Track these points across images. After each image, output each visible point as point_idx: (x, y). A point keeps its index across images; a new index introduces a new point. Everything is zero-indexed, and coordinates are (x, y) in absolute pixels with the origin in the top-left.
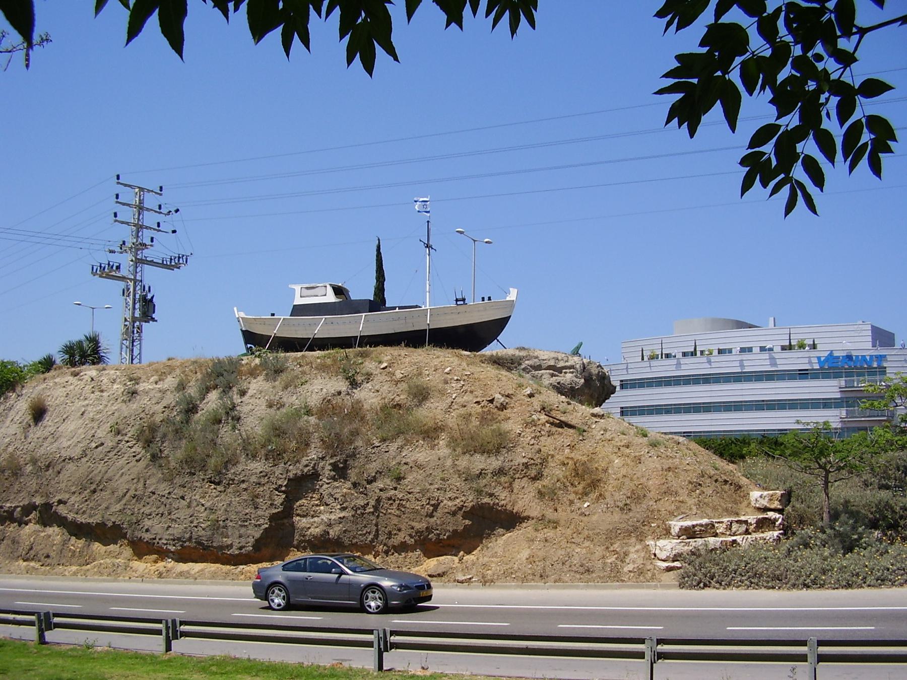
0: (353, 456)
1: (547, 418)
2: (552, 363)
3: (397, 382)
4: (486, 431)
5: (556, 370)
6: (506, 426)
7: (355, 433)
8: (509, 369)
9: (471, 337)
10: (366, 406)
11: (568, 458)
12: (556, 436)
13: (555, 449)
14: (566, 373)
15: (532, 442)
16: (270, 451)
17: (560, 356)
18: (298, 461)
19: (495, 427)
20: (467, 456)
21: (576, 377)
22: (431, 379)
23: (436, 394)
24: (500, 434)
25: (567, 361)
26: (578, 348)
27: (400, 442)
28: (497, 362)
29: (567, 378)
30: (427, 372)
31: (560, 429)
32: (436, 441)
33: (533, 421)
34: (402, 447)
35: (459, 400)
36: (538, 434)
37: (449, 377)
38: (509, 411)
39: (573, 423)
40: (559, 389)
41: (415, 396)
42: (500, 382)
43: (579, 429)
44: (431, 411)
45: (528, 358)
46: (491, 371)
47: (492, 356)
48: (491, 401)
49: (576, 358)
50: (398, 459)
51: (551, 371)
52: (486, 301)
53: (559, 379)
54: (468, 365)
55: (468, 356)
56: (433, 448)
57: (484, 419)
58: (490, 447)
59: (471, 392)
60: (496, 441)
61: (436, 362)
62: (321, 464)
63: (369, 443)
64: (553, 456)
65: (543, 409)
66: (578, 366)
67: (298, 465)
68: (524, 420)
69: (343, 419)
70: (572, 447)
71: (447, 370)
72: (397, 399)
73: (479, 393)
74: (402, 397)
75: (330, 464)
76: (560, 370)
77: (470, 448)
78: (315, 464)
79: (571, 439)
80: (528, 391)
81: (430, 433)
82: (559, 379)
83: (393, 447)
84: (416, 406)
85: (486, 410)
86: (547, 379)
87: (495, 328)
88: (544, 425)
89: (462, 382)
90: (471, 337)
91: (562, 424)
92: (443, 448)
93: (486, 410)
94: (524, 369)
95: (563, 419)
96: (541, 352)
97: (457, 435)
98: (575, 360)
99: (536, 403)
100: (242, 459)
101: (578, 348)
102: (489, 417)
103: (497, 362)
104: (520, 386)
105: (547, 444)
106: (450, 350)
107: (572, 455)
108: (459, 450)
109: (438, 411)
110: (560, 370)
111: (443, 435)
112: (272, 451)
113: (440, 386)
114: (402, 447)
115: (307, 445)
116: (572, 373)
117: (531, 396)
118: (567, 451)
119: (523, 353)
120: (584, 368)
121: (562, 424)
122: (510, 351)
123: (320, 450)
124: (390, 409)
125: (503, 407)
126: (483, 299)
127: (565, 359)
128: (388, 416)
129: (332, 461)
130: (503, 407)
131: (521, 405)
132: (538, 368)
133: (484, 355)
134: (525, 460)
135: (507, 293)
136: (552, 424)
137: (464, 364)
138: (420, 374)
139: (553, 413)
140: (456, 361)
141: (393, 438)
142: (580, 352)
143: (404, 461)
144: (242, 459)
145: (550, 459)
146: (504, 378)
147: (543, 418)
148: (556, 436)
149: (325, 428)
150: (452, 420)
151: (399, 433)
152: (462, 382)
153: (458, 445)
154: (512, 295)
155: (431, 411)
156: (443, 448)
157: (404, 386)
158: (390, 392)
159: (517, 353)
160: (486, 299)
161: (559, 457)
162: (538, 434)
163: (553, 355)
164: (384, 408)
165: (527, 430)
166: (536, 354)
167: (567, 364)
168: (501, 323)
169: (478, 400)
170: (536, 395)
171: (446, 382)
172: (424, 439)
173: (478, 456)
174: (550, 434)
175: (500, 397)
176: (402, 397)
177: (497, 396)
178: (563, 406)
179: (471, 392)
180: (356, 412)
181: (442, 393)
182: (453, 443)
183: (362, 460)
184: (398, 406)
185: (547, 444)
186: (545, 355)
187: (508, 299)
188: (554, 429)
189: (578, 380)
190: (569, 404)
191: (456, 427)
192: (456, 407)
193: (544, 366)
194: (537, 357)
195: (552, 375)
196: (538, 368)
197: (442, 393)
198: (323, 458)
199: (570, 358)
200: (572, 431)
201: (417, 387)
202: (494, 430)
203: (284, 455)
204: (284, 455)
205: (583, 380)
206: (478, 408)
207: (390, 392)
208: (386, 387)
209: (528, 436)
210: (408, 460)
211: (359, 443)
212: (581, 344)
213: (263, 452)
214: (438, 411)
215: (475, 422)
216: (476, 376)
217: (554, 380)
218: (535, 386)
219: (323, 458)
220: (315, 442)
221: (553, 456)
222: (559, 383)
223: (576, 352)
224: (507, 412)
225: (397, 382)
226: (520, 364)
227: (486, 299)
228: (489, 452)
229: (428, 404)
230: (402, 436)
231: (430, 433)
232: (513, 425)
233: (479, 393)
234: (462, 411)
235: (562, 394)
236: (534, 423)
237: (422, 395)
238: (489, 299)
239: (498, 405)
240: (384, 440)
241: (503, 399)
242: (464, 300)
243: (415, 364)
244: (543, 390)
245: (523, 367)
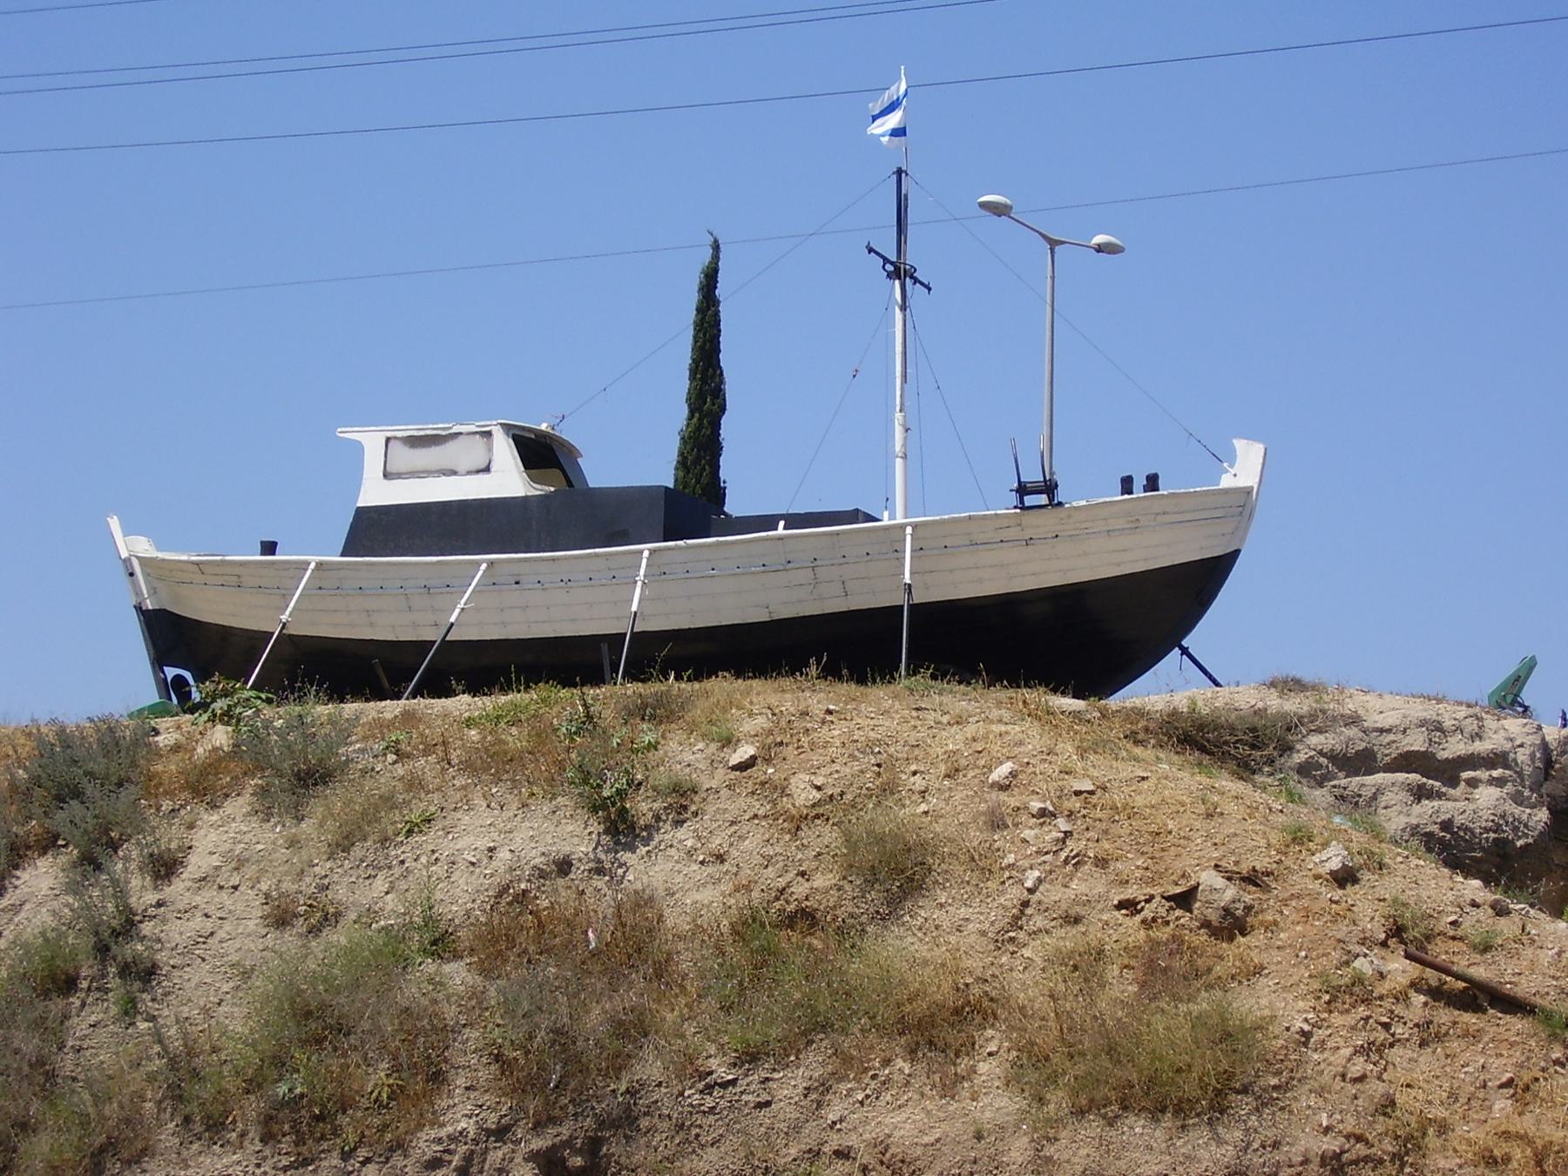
0: (626, 1121)
1: (1414, 970)
2: (1416, 742)
3: (798, 823)
4: (1171, 1025)
5: (1434, 771)
6: (1251, 1003)
7: (632, 1030)
8: (1245, 770)
9: (1080, 639)
10: (675, 920)
11: (1506, 1135)
12: (1455, 1045)
13: (1453, 1096)
14: (1473, 783)
15: (1358, 1067)
16: (283, 1104)
17: (1449, 715)
18: (399, 1146)
19: (1203, 1004)
20: (1093, 1127)
21: (1518, 799)
22: (937, 809)
23: (958, 869)
24: (1227, 1036)
25: (1477, 736)
26: (1518, 681)
27: (813, 1064)
28: (1197, 738)
29: (1482, 804)
30: (918, 782)
31: (1469, 1018)
32: (964, 1064)
33: (1358, 980)
34: (824, 1087)
35: (1052, 894)
36: (1381, 1035)
37: (1011, 800)
38: (1257, 938)
39: (1524, 987)
40: (1451, 849)
41: (872, 878)
42: (1218, 825)
43: (1548, 1017)
44: (942, 938)
45: (1319, 721)
46: (1176, 780)
47: (1175, 713)
48: (1184, 900)
49: (1514, 725)
50: (810, 1135)
51: (1414, 777)
52: (1139, 493)
53: (1446, 808)
54: (1082, 752)
55: (1076, 715)
56: (948, 1089)
57: (1160, 972)
58: (1190, 1089)
59: (1102, 862)
60: (1209, 1062)
61: (954, 740)
62: (496, 1156)
63: (691, 1070)
64: (1443, 1128)
65: (1397, 931)
66: (1522, 756)
67: (397, 1160)
68: (1322, 975)
69: (583, 970)
70: (1520, 1090)
71: (1001, 772)
72: (800, 889)
73: (1131, 865)
74: (820, 881)
75: (533, 1157)
76: (1449, 772)
77: (1105, 1090)
78: (468, 1158)
79: (1518, 1056)
80: (1333, 858)
81: (938, 1031)
82: (1446, 808)
83: (790, 1085)
84: (882, 918)
85: (1163, 934)
86: (1399, 808)
87: (1165, 605)
88: (1401, 997)
89: (1062, 823)
90: (1080, 639)
91: (1480, 997)
92: (991, 1094)
93: (1163, 934)
94: (1304, 770)
95: (1480, 972)
96: (1372, 701)
97: (1047, 1038)
98: (1507, 732)
99: (1367, 907)
100: (167, 1136)
101: (1518, 681)
102: (1178, 964)
103: (1197, 738)
104: (1300, 837)
105: (1420, 1078)
106: (1000, 693)
107: (1526, 1124)
108: (1058, 1101)
109: (970, 937)
110: (1449, 772)
111: (993, 1039)
112: (294, 1102)
113: (975, 837)
114: (824, 1087)
115: (437, 1078)
116: (1499, 782)
117: (1345, 877)
118: (1502, 1105)
119: (1294, 705)
120: (1549, 763)
121: (1480, 997)
122: (1243, 696)
123: (486, 1098)
124: (773, 934)
125: (1232, 925)
126: (1127, 485)
127: (1471, 726)
128: (765, 960)
129: (538, 1144)
130: (1232, 925)
131: (1307, 915)
132: (1362, 762)
133: (1140, 713)
134: (1331, 1144)
135: (1222, 458)
136: (1437, 994)
137: (1067, 748)
138: (889, 789)
139: (1440, 951)
140: (1034, 738)
141: (787, 1052)
142: (1527, 696)
143: (834, 1142)
144: (167, 1136)
145: (1432, 1140)
146: (1230, 807)
147: (1399, 968)
148: (1455, 1045)
149: (509, 1013)
150: (1027, 976)
151: (813, 1027)
152: (1062, 823)
153: (1053, 1079)
154: (1245, 467)
155: (942, 938)
156: (991, 1094)
157: (825, 836)
158: (769, 861)
159: (1274, 702)
160: (1139, 482)
161: (1471, 1132)
162: (1381, 1035)
163: (1419, 710)
164: (746, 927)
165: (1337, 1019)
166: (1350, 706)
167: (1480, 747)
168: (1201, 582)
169: (1130, 892)
170: (1365, 876)
171: (997, 822)
172: (912, 1053)
173: (1136, 1126)
174: (1428, 1036)
175: (1219, 882)
176: (820, 881)
177: (1209, 879)
178: (1478, 922)
179: (1102, 862)
180: (636, 943)
181: (983, 865)
182: (1033, 1068)
183: (662, 1140)
184: (804, 918)
185: (1420, 1078)
186: (1388, 710)
187: (1226, 482)
188: (1444, 1016)
189: (1522, 813)
190: (1500, 911)
191: (1042, 1004)
192: (1039, 921)
193: (1385, 754)
194: (1354, 720)
195: (1420, 794)
196: (1362, 762)
197: (983, 865)
198: (501, 1133)
199: (1490, 722)
200: (1517, 1024)
201: (880, 840)
202: (1198, 1021)
203: (342, 1120)
204: (342, 1120)
205: (1543, 815)
206: (1131, 929)
207: (769, 861)
208: (753, 842)
209: (1338, 1050)
210: (852, 1140)
211: (650, 1068)
212: (1530, 665)
213: (253, 1106)
214: (970, 937)
215: (1121, 985)
216: (1118, 799)
217: (1426, 813)
218: (1359, 839)
219: (501, 1133)
220: (469, 1065)
221: (1443, 1128)
222: (1446, 825)
223: (1510, 699)
224: (1250, 946)
225: (798, 823)
226: (1286, 748)
227: (1139, 482)
228: (1182, 1109)
229: (925, 911)
230: (823, 1043)
231: (938, 1031)
232: (1276, 1001)
233: (1131, 865)
234: (1067, 939)
235: (1468, 874)
236: (1359, 992)
237: (899, 873)
238: (1152, 483)
239: (1213, 916)
240: (749, 1057)
241: (1230, 892)
242: (1049, 488)
243: (869, 747)
244: (1390, 854)
245: (1299, 758)
